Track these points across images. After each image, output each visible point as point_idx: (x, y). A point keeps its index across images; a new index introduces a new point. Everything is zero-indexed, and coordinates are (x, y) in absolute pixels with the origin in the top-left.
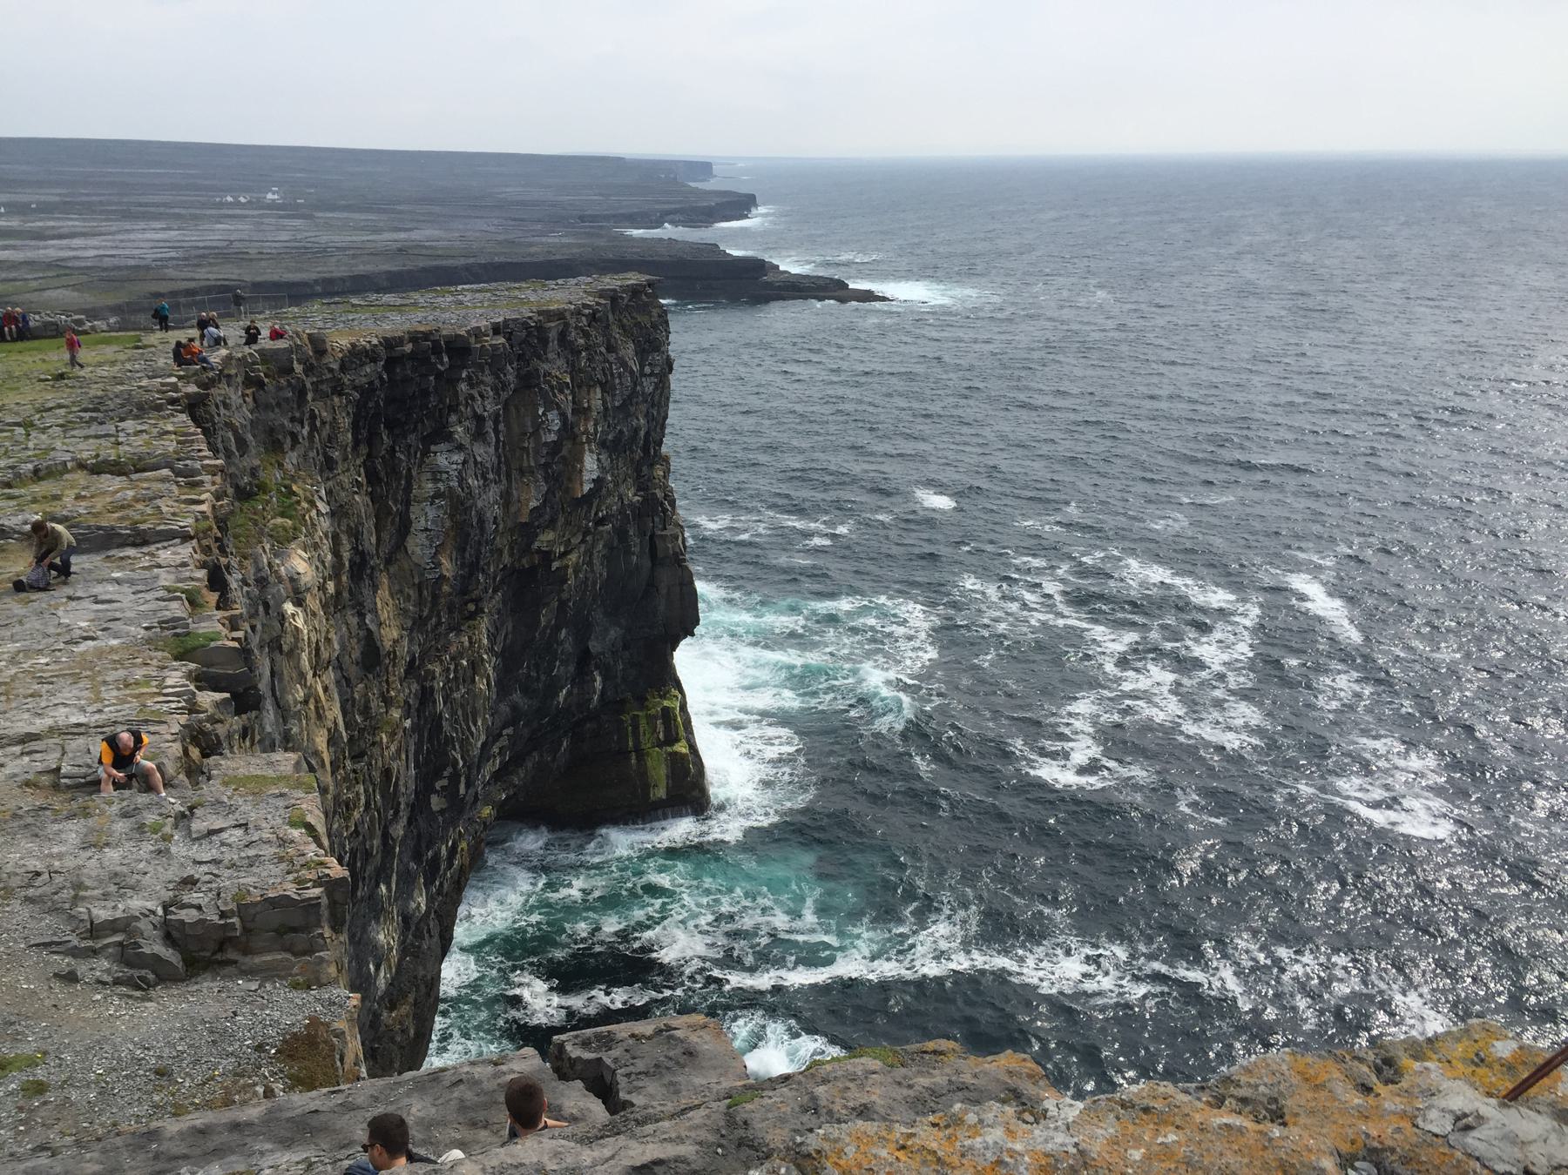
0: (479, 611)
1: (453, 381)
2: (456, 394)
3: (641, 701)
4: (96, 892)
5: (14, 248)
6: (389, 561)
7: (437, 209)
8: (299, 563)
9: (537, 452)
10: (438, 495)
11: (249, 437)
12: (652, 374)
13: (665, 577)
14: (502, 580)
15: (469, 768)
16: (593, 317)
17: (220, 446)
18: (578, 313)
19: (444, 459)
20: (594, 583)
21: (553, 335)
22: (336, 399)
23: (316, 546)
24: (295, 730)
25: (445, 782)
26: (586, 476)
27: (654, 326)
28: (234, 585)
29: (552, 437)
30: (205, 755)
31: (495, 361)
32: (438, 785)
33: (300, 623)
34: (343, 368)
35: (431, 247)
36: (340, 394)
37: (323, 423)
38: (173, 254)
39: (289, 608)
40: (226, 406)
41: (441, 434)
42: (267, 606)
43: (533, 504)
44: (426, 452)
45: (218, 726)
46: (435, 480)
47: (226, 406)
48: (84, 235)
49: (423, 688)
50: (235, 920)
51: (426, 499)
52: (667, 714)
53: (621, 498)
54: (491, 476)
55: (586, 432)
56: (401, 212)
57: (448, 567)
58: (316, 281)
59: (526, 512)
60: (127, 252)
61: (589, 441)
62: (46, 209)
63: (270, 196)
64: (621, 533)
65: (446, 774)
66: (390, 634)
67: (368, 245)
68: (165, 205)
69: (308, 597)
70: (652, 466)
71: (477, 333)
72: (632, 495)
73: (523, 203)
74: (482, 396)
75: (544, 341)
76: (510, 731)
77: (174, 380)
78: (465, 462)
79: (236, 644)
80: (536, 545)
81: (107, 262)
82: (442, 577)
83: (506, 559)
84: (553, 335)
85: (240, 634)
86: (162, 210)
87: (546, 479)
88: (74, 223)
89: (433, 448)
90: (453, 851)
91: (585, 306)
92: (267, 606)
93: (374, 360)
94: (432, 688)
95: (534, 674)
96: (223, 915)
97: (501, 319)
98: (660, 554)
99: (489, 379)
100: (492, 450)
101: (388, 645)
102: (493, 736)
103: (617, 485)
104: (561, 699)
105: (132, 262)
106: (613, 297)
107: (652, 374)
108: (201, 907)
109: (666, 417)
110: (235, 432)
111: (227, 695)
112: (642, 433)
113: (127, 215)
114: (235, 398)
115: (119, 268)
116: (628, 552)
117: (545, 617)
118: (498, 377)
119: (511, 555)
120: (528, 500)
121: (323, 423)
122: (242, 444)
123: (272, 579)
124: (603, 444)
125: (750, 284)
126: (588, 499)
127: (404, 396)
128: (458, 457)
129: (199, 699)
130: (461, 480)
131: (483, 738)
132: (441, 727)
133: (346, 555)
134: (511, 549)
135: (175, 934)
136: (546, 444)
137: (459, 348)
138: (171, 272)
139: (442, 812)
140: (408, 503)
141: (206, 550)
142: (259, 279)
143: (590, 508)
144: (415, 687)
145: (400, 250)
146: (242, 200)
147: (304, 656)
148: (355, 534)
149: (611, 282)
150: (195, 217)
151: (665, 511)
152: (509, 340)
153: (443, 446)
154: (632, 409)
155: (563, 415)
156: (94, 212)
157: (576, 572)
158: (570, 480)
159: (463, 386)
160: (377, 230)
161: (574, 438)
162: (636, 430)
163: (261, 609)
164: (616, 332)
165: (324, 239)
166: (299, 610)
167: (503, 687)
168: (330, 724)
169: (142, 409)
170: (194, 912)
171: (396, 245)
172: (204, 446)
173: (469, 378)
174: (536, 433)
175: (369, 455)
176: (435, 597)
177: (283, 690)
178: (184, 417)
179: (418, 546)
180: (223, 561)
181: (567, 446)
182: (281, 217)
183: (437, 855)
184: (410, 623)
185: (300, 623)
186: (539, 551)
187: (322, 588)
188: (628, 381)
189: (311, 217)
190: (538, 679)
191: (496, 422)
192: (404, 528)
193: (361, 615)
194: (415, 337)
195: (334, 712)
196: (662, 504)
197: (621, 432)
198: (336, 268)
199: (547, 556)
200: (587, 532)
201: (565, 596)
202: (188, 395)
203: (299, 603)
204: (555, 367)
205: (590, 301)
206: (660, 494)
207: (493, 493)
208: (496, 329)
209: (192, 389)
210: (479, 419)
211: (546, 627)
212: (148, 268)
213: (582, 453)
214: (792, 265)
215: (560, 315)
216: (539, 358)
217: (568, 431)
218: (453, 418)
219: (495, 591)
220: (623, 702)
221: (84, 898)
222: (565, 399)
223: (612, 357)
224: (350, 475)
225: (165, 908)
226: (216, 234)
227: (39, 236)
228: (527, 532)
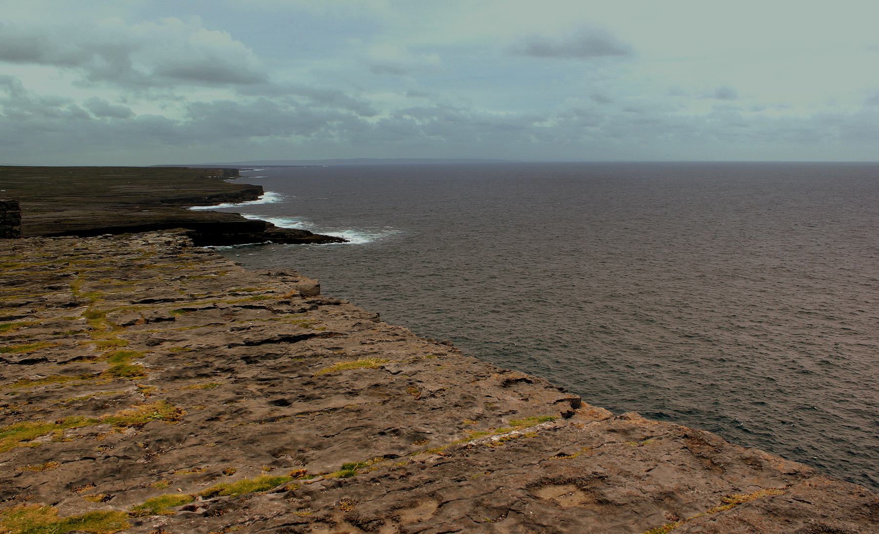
7: (79, 199)
35: (74, 220)
67: (37, 220)
73: (127, 194)
125: (257, 234)
145: (55, 222)
160: (44, 212)
171: (53, 219)
214: (279, 223)
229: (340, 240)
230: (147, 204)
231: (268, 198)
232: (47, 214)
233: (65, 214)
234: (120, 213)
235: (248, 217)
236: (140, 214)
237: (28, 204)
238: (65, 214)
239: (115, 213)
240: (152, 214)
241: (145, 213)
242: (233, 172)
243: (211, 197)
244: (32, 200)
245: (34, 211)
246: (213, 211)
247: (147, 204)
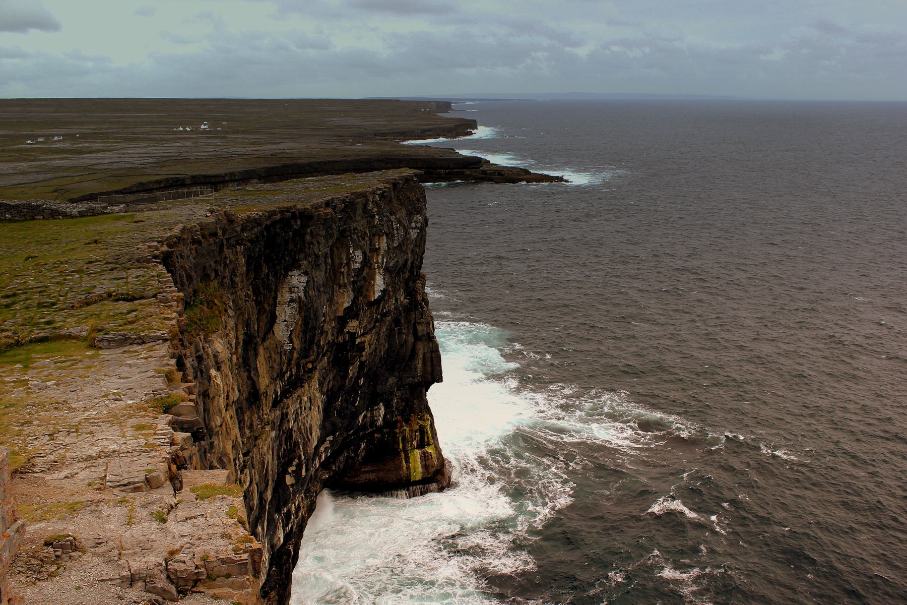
0: (314, 368)
1: (303, 236)
2: (304, 241)
3: (407, 421)
4: (130, 551)
5: (66, 158)
6: (264, 340)
8: (219, 345)
9: (349, 274)
10: (292, 301)
11: (193, 274)
12: (416, 227)
13: (421, 348)
14: (327, 351)
15: (308, 460)
16: (382, 196)
17: (178, 280)
18: (374, 193)
19: (297, 280)
20: (380, 352)
21: (360, 208)
22: (238, 247)
23: (227, 335)
24: (216, 443)
25: (294, 468)
27: (418, 200)
28: (188, 365)
29: (358, 266)
30: (179, 468)
31: (327, 223)
32: (290, 469)
33: (219, 381)
34: (243, 230)
35: (290, 153)
36: (240, 245)
37: (231, 261)
38: (150, 161)
39: (213, 372)
40: (182, 257)
41: (294, 265)
42: (202, 372)
43: (347, 305)
44: (286, 275)
45: (185, 452)
46: (291, 292)
47: (182, 257)
48: (103, 151)
49: (283, 414)
50: (202, 570)
51: (285, 303)
52: (422, 430)
53: (396, 300)
54: (322, 289)
55: (377, 262)
56: (273, 133)
57: (297, 344)
58: (226, 174)
59: (342, 309)
60: (126, 160)
61: (379, 268)
62: (84, 137)
63: (203, 127)
64: (397, 322)
65: (294, 463)
66: (264, 382)
67: (254, 152)
68: (147, 133)
69: (223, 365)
70: (414, 282)
71: (317, 207)
72: (403, 299)
73: (341, 127)
74: (318, 243)
75: (354, 210)
76: (330, 438)
77: (156, 244)
78: (307, 282)
79: (192, 404)
80: (346, 329)
81: (115, 166)
82: (294, 348)
83: (330, 338)
84: (360, 208)
85: (193, 397)
86: (145, 136)
87: (353, 290)
88: (99, 145)
89: (290, 273)
90: (298, 509)
91: (378, 189)
92: (202, 372)
93: (260, 224)
94: (287, 414)
95: (345, 405)
96: (197, 567)
97: (330, 198)
98: (420, 335)
99: (323, 233)
100: (323, 274)
101: (262, 388)
102: (321, 441)
103: (394, 292)
104: (361, 418)
105: (128, 166)
106: (395, 185)
107: (416, 227)
108: (186, 563)
109: (423, 253)
110: (186, 271)
111: (189, 434)
112: (409, 262)
113: (127, 140)
114: (186, 252)
115: (121, 169)
116: (400, 333)
117: (352, 371)
118: (327, 231)
119: (333, 335)
120: (343, 303)
121: (231, 261)
122: (189, 278)
123: (205, 356)
124: (387, 270)
125: (474, 172)
126: (378, 302)
127: (277, 245)
128: (304, 279)
129: (175, 437)
130: (306, 292)
131: (315, 443)
132: (291, 436)
133: (241, 337)
134: (333, 332)
135: (172, 577)
136: (354, 270)
137: (306, 217)
138: (148, 171)
139: (292, 485)
140: (275, 306)
141: (174, 346)
142: (195, 173)
143: (379, 306)
144: (278, 413)
146: (188, 129)
147: (221, 400)
148: (247, 325)
149: (394, 174)
150: (161, 139)
151: (422, 308)
152: (334, 209)
153: (296, 272)
154: (404, 248)
155: (364, 254)
156: (109, 138)
157: (370, 345)
158: (368, 290)
159: (308, 237)
162: (406, 261)
163: (199, 373)
164: (395, 203)
165: (231, 150)
166: (218, 373)
167: (327, 411)
168: (233, 437)
169: (141, 262)
170: (182, 565)
172: (172, 284)
173: (311, 232)
174: (348, 264)
175: (255, 279)
176: (290, 360)
177: (209, 419)
178: (161, 267)
179: (281, 332)
180: (183, 352)
181: (366, 270)
182: (208, 138)
183: (289, 511)
184: (275, 375)
185: (219, 381)
186: (348, 332)
187: (230, 360)
188: (402, 232)
189: (225, 138)
190: (347, 408)
191: (325, 258)
192: (273, 319)
193: (249, 372)
194: (282, 211)
195: (236, 431)
196: (421, 304)
197: (397, 261)
198: (237, 167)
199: (353, 336)
200: (377, 321)
201: (363, 359)
202: (163, 252)
203: (218, 369)
204: (360, 224)
206: (419, 298)
207: (324, 298)
208: (327, 204)
209: (165, 248)
210: (317, 256)
211: (352, 377)
212: (136, 168)
213: (374, 274)
215: (363, 195)
216: (351, 219)
217: (367, 262)
218: (302, 256)
219: (324, 356)
220: (397, 421)
221: (125, 555)
222: (366, 243)
223: (393, 218)
224: (244, 291)
225: (166, 563)
226: (172, 149)
227: (80, 152)
228: (342, 322)
229: (560, 179)
230: (360, 137)
231: (482, 132)
232: (265, 147)
233: (281, 146)
234: (334, 146)
235: (465, 153)
236: (353, 147)
237: (247, 136)
238: (281, 146)
239: (329, 146)
240: (365, 147)
241: (359, 146)
242: (445, 105)
243: (424, 131)
244: (251, 133)
245: (252, 143)
246: (427, 146)
247: (360, 137)
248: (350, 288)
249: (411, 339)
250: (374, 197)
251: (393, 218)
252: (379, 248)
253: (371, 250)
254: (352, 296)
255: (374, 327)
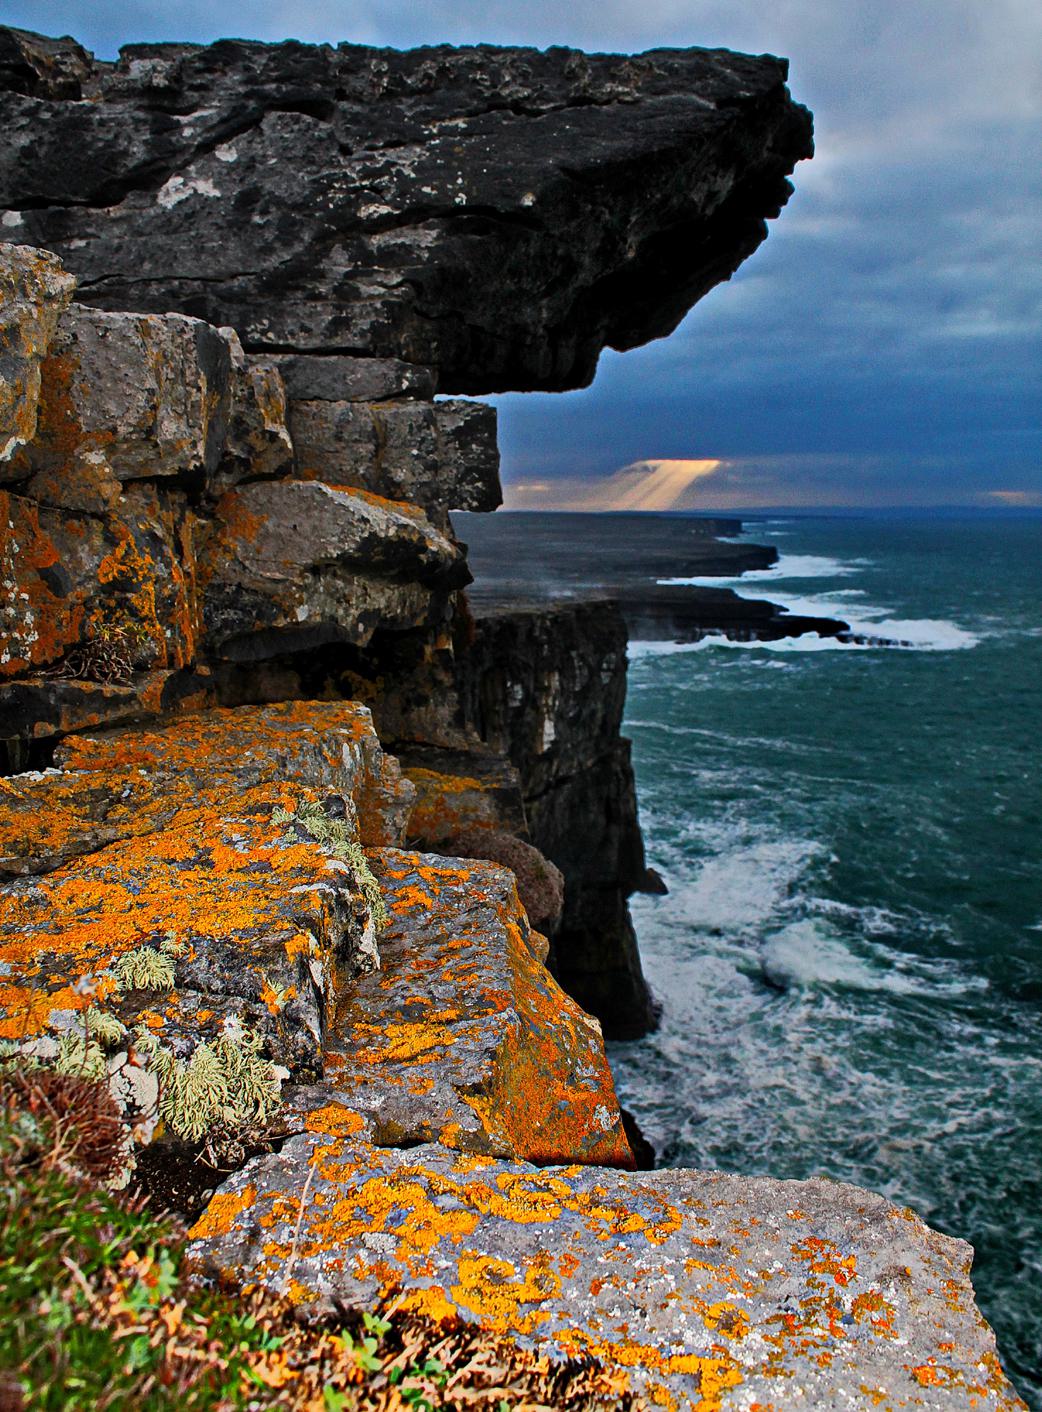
12: (608, 670)
18: (543, 617)
26: (546, 738)
29: (517, 704)
55: (547, 705)
107: (608, 670)
126: (548, 757)
143: (551, 764)
155: (525, 689)
161: (537, 708)
162: (593, 713)
174: (505, 702)
188: (586, 672)
205: (554, 609)
213: (543, 721)
215: (528, 617)
217: (530, 700)
248: (507, 732)
249: (602, 820)
250: (543, 623)
251: (574, 654)
252: (549, 687)
253: (536, 689)
254: (510, 742)
255: (545, 792)
